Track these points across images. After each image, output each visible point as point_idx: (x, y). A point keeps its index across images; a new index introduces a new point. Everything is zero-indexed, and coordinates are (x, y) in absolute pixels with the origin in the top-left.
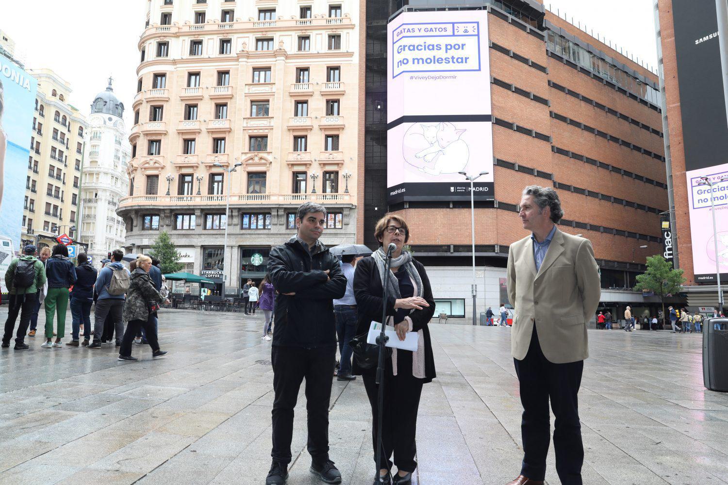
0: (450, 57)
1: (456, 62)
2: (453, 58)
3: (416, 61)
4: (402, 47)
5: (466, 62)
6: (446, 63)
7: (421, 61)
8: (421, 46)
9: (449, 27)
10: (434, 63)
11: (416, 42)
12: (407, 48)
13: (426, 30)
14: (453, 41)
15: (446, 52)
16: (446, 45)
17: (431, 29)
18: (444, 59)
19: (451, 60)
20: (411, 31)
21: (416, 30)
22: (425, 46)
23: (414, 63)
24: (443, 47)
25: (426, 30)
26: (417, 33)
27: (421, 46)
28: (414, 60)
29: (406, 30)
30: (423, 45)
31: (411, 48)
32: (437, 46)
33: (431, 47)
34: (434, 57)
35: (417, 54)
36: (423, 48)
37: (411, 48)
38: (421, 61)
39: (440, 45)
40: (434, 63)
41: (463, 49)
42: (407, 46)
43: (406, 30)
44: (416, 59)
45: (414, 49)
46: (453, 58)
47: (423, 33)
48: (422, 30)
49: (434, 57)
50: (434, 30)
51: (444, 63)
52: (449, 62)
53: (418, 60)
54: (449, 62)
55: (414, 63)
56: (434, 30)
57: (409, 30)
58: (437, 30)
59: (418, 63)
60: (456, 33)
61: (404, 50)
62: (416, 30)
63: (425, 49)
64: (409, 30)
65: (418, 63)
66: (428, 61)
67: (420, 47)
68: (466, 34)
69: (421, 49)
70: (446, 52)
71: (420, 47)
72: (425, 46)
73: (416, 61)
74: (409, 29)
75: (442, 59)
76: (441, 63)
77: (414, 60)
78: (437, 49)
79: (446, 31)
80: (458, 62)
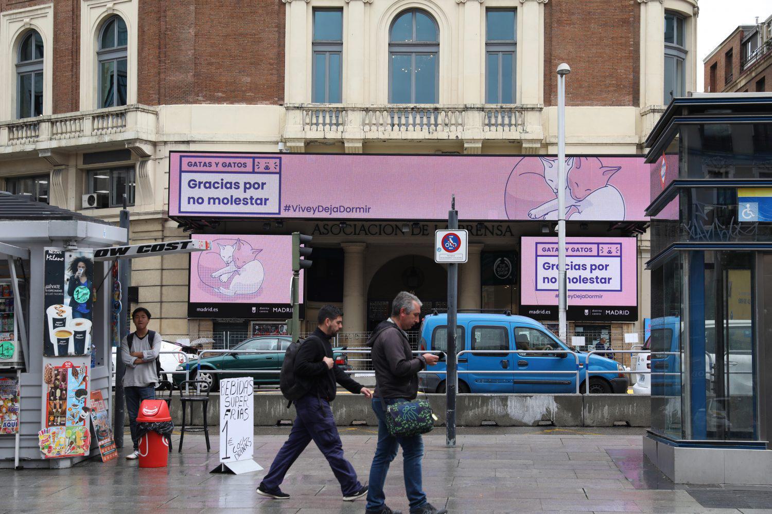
0: (249, 198)
1: (255, 204)
2: (252, 198)
3: (212, 201)
4: (197, 183)
5: (265, 204)
6: (244, 204)
7: (217, 201)
8: (218, 183)
9: (249, 162)
10: (232, 204)
11: (213, 178)
12: (202, 185)
13: (224, 165)
14: (252, 179)
15: (245, 192)
16: (245, 184)
17: (230, 163)
18: (242, 199)
19: (249, 201)
20: (208, 165)
21: (214, 165)
22: (222, 183)
23: (209, 203)
24: (242, 186)
25: (224, 165)
26: (214, 168)
27: (218, 183)
28: (209, 199)
29: (202, 164)
30: (220, 181)
31: (207, 185)
32: (235, 184)
33: (228, 185)
34: (232, 196)
35: (213, 193)
36: (220, 185)
37: (207, 185)
38: (217, 201)
39: (238, 183)
40: (232, 204)
41: (262, 188)
42: (202, 182)
43: (202, 164)
44: (213, 198)
45: (210, 187)
46: (252, 198)
47: (220, 168)
48: (220, 165)
49: (232, 196)
50: (233, 165)
51: (242, 204)
52: (247, 203)
53: (214, 199)
54: (247, 203)
55: (209, 203)
56: (233, 165)
57: (205, 165)
58: (236, 164)
59: (214, 203)
60: (256, 170)
61: (199, 187)
62: (214, 165)
63: (222, 188)
64: (205, 165)
65: (214, 203)
66: (224, 201)
67: (216, 185)
68: (267, 171)
69: (218, 187)
70: (245, 192)
71: (216, 185)
72: (222, 183)
73: (212, 201)
74: (205, 163)
75: (240, 200)
76: (239, 204)
77: (209, 199)
78: (235, 188)
79: (246, 166)
80: (257, 204)
